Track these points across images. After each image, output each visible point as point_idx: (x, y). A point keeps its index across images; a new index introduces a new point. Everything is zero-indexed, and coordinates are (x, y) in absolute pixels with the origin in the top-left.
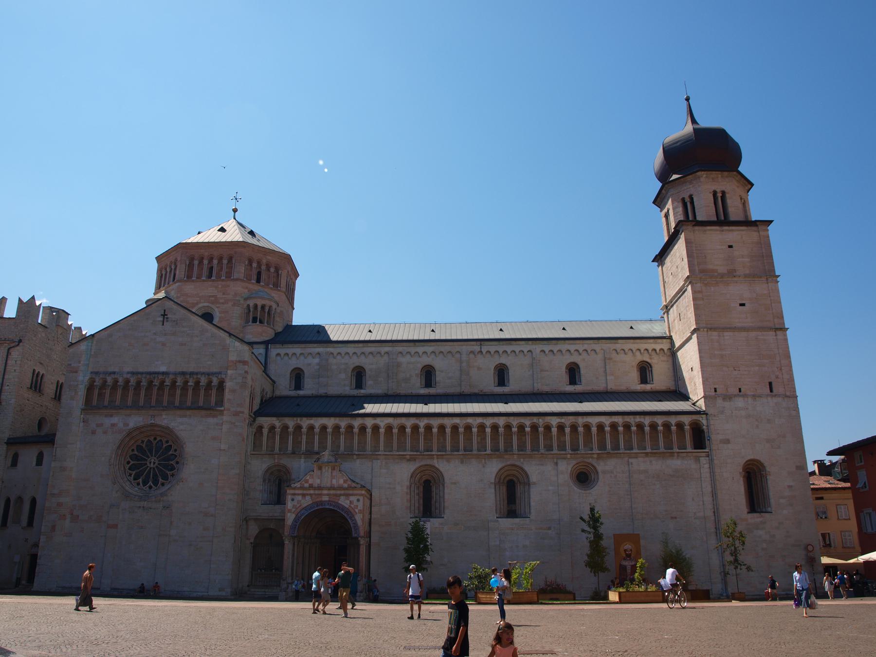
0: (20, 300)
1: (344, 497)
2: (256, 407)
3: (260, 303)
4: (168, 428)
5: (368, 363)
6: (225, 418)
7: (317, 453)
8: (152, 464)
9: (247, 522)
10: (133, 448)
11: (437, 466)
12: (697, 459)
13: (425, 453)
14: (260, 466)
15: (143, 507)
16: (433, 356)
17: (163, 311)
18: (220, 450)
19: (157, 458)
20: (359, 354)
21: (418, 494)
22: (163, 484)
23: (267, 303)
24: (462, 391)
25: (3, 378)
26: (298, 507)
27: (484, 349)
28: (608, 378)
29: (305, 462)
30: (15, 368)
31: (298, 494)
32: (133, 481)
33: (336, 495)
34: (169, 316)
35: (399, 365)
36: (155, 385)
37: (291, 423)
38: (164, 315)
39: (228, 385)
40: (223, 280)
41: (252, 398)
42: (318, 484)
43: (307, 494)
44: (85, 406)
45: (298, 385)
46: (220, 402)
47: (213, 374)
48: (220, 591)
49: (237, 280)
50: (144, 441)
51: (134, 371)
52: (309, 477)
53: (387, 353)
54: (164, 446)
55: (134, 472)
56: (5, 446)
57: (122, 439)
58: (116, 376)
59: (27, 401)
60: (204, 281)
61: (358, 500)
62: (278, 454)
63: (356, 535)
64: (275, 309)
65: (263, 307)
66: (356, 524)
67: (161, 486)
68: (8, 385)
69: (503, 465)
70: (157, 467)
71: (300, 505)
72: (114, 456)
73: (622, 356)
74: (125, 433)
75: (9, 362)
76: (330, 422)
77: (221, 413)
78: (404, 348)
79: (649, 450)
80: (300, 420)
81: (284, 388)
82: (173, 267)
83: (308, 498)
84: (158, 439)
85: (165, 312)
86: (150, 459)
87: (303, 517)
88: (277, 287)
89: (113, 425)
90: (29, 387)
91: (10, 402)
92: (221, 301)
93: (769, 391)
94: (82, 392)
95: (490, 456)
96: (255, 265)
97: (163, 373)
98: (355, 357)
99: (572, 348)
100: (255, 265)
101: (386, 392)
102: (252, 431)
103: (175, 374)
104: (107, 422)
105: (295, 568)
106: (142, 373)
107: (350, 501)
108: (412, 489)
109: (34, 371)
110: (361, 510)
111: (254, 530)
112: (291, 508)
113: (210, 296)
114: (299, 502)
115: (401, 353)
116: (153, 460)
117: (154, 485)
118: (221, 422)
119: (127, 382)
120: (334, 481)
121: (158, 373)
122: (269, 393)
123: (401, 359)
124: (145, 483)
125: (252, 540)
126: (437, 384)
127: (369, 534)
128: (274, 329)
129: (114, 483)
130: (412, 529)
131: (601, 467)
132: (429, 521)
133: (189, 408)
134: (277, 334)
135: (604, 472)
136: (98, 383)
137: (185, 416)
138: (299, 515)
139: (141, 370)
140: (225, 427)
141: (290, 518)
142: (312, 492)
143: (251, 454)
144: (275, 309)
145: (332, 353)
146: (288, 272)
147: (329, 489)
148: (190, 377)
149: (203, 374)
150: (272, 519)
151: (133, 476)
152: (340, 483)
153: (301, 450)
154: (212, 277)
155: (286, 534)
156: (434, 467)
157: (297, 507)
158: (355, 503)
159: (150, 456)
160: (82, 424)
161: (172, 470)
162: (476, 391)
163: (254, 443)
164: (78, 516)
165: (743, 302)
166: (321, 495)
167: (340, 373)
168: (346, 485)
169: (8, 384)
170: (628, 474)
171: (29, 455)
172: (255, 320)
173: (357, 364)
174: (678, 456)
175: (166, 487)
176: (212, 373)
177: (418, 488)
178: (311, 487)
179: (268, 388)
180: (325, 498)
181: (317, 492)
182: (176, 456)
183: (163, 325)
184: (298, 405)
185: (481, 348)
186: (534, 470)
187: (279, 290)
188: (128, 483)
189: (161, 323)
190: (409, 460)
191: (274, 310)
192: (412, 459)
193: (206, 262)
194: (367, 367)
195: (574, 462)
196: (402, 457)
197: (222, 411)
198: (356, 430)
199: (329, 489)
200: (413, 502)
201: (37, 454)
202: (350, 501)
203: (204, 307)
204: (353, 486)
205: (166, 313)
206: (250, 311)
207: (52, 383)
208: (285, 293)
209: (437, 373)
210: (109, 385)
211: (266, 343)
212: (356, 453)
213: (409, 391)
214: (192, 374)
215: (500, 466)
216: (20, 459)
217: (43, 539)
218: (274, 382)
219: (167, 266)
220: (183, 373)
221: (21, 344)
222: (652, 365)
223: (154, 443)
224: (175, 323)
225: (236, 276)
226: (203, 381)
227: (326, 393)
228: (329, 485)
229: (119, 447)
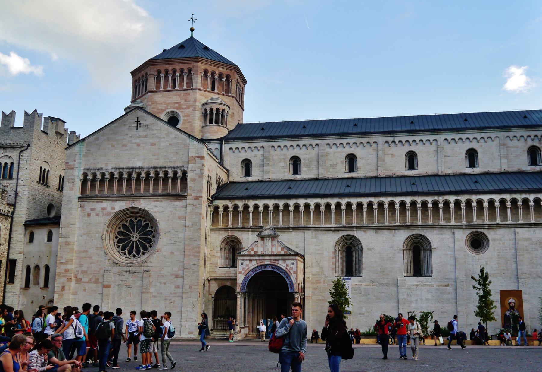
0: (26, 112)
1: (282, 261)
2: (213, 192)
3: (215, 107)
4: (145, 210)
5: (301, 153)
6: (189, 201)
7: (261, 227)
8: (135, 238)
9: (209, 281)
10: (119, 226)
11: (356, 235)
13: (347, 226)
14: (217, 238)
15: (129, 271)
16: (354, 146)
17: (136, 118)
18: (186, 226)
19: (138, 233)
21: (342, 258)
22: (143, 254)
23: (221, 107)
24: (379, 174)
25: (18, 175)
26: (247, 270)
29: (252, 234)
32: (120, 252)
34: (141, 122)
35: (327, 154)
36: (134, 177)
37: (240, 204)
38: (137, 121)
39: (190, 175)
40: (185, 90)
41: (209, 184)
42: (262, 252)
43: (253, 260)
44: (81, 194)
45: (248, 173)
46: (184, 188)
47: (177, 167)
48: (189, 334)
49: (196, 89)
50: (128, 221)
51: (117, 167)
52: (254, 246)
53: (317, 145)
54: (143, 224)
55: (121, 245)
56: (24, 227)
57: (111, 220)
58: (103, 171)
59: (38, 192)
60: (169, 91)
61: (293, 264)
62: (231, 229)
63: (291, 291)
64: (228, 112)
65: (218, 110)
66: (291, 282)
67: (142, 255)
68: (22, 180)
70: (138, 240)
71: (247, 268)
72: (105, 233)
74: (112, 215)
75: (21, 162)
76: (271, 203)
77: (185, 197)
78: (332, 140)
80: (248, 202)
81: (237, 175)
82: (144, 80)
83: (254, 262)
84: (138, 219)
85: (138, 119)
86: (133, 234)
87: (250, 277)
88: (229, 93)
89: (103, 209)
90: (38, 181)
91: (25, 193)
92: (184, 107)
94: (78, 185)
96: (209, 75)
97: (139, 168)
98: (291, 149)
100: (209, 75)
101: (317, 177)
102: (211, 211)
103: (149, 168)
104: (99, 206)
105: (246, 317)
106: (123, 168)
107: (287, 264)
108: (337, 254)
109: (41, 168)
110: (295, 271)
111: (215, 287)
112: (241, 270)
114: (247, 265)
115: (328, 144)
116: (135, 235)
117: (137, 255)
118: (185, 204)
119: (112, 174)
120: (274, 249)
121: (135, 168)
122: (224, 180)
123: (328, 149)
124: (130, 253)
125: (213, 295)
126: (358, 169)
128: (227, 128)
129: (106, 254)
130: (335, 286)
132: (350, 279)
133: (160, 195)
134: (230, 132)
136: (90, 177)
137: (158, 201)
138: (248, 275)
139: (122, 166)
140: (189, 209)
141: (240, 279)
142: (257, 258)
143: (210, 229)
144: (228, 112)
145: (273, 146)
146: (237, 80)
147: (270, 255)
148: (160, 170)
149: (169, 168)
150: (228, 279)
151: (120, 247)
152: (278, 250)
153: (249, 225)
154: (175, 87)
155: (238, 290)
157: (246, 269)
159: (133, 232)
160: (80, 209)
162: (390, 174)
163: (212, 220)
164: (81, 279)
167: (280, 162)
168: (283, 253)
169: (22, 179)
171: (41, 234)
173: (294, 154)
175: (146, 255)
176: (177, 167)
177: (342, 253)
178: (256, 255)
179: (223, 176)
180: (267, 263)
181: (261, 258)
182: (152, 232)
183: (137, 129)
184: (247, 189)
188: (117, 253)
189: (136, 128)
190: (334, 231)
191: (226, 112)
192: (336, 230)
193: (170, 75)
194: (301, 157)
196: (328, 229)
197: (186, 196)
198: (292, 208)
199: (270, 255)
200: (337, 264)
201: (47, 233)
202: (287, 264)
203: (170, 112)
204: (288, 253)
205: (139, 120)
206: (207, 114)
207: (56, 177)
208: (235, 98)
209: (358, 160)
210: (98, 179)
211: (221, 140)
212: (292, 226)
213: (336, 176)
214: (161, 168)
216: (36, 237)
217: (56, 296)
218: (228, 171)
219: (140, 79)
220: (155, 168)
221: (29, 148)
223: (135, 222)
224: (146, 127)
225: (194, 86)
226: (171, 174)
227: (269, 179)
228: (270, 253)
229: (108, 226)
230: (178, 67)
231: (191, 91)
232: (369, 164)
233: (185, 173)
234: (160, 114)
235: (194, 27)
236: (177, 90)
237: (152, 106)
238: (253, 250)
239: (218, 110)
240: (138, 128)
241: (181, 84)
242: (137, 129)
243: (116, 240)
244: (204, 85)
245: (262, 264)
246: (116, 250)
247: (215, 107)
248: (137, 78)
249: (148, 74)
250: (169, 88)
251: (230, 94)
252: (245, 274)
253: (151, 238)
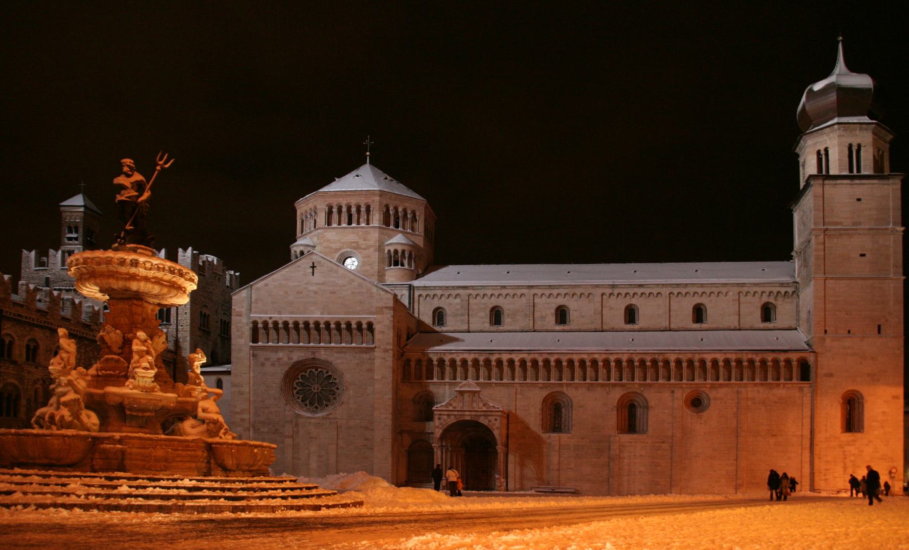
11: (566, 392)
12: (801, 389)
27: (616, 292)
30: (186, 311)
31: (444, 415)
33: (476, 415)
54: (325, 376)
61: (496, 420)
69: (626, 392)
83: (452, 417)
84: (319, 370)
95: (614, 385)
113: (352, 242)
131: (712, 394)
135: (715, 399)
142: (456, 413)
156: (563, 393)
158: (493, 421)
161: (334, 394)
166: (464, 415)
168: (485, 409)
170: (736, 401)
172: (396, 264)
174: (784, 386)
180: (468, 418)
181: (460, 413)
182: (336, 384)
185: (613, 290)
186: (652, 396)
192: (544, 386)
195: (689, 391)
199: (471, 411)
207: (217, 322)
209: (571, 312)
215: (622, 393)
222: (777, 306)
223: (316, 372)
231: (372, 230)
232: (582, 317)
237: (325, 244)
238: (451, 405)
243: (295, 391)
244: (386, 222)
245: (461, 419)
246: (295, 402)
251: (417, 233)
252: (443, 429)
253: (336, 390)
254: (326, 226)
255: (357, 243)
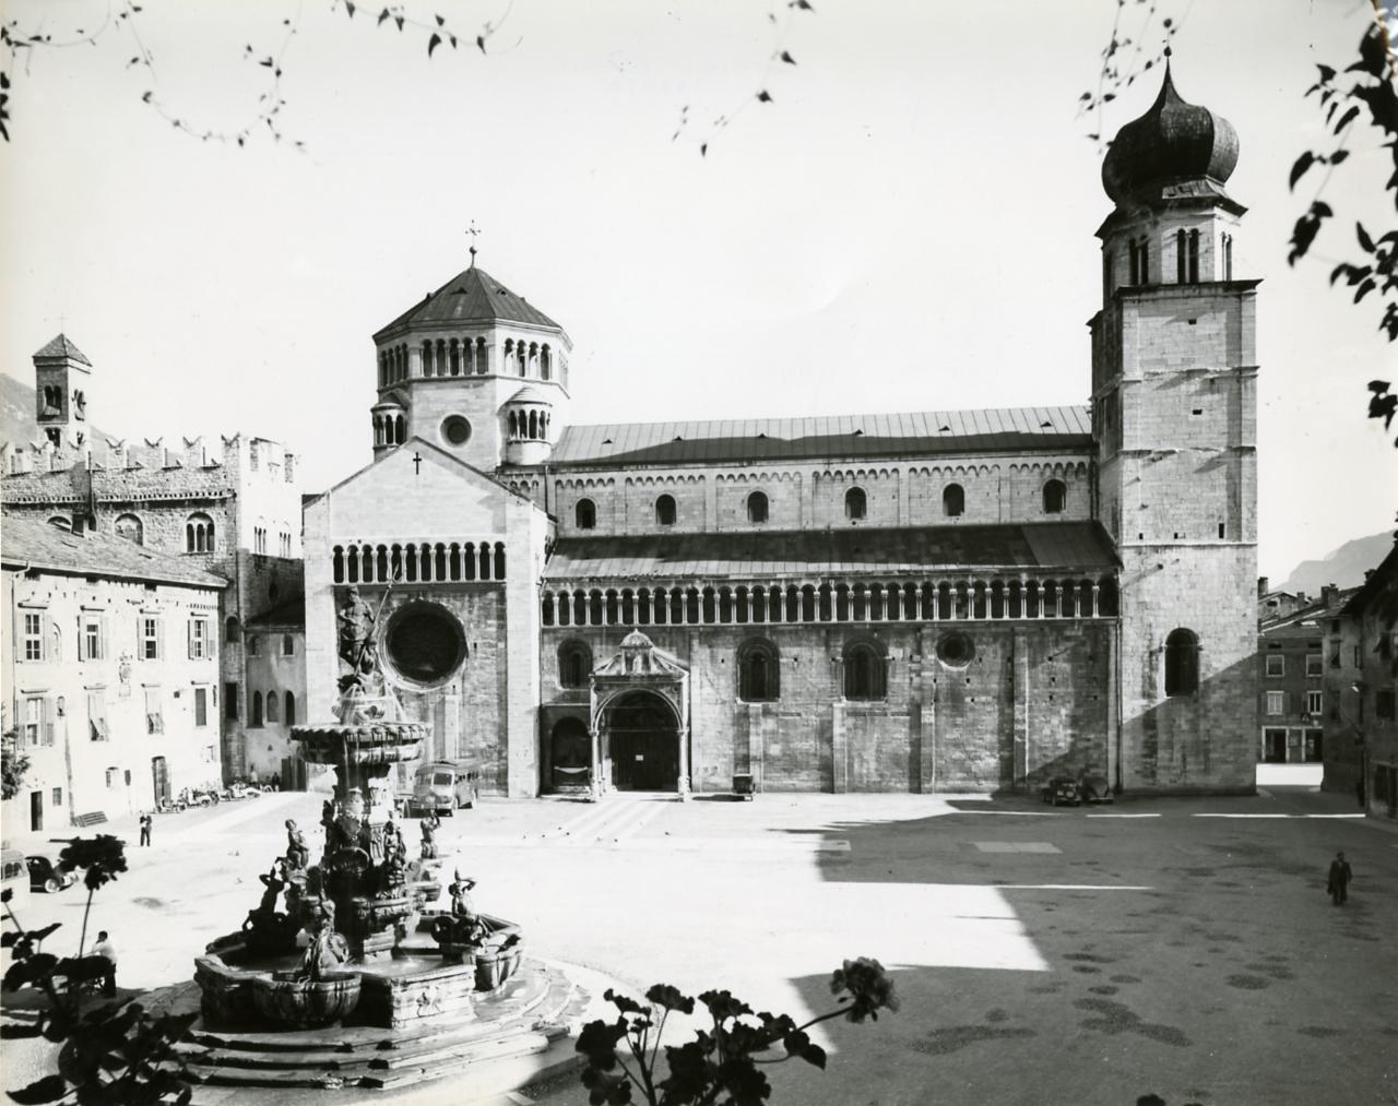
5: (680, 492)
20: (665, 479)
23: (538, 409)
27: (834, 468)
28: (1002, 506)
38: (417, 460)
46: (501, 573)
49: (494, 377)
53: (702, 477)
65: (533, 413)
73: (1025, 472)
79: (1041, 617)
81: (572, 530)
92: (475, 407)
93: (1217, 534)
96: (515, 346)
99: (954, 464)
100: (515, 346)
127: (689, 724)
165: (1199, 408)
183: (417, 473)
187: (551, 384)
194: (678, 497)
230: (460, 336)
233: (500, 546)
234: (435, 421)
235: (475, 249)
236: (462, 379)
239: (533, 413)
240: (420, 471)
241: (468, 370)
242: (417, 473)
247: (528, 409)
248: (386, 347)
249: (410, 346)
250: (448, 374)
254: (423, 376)
255: (466, 401)
